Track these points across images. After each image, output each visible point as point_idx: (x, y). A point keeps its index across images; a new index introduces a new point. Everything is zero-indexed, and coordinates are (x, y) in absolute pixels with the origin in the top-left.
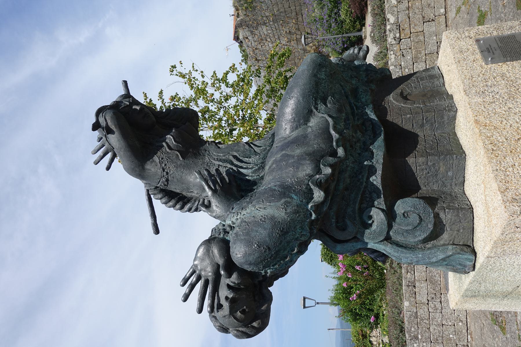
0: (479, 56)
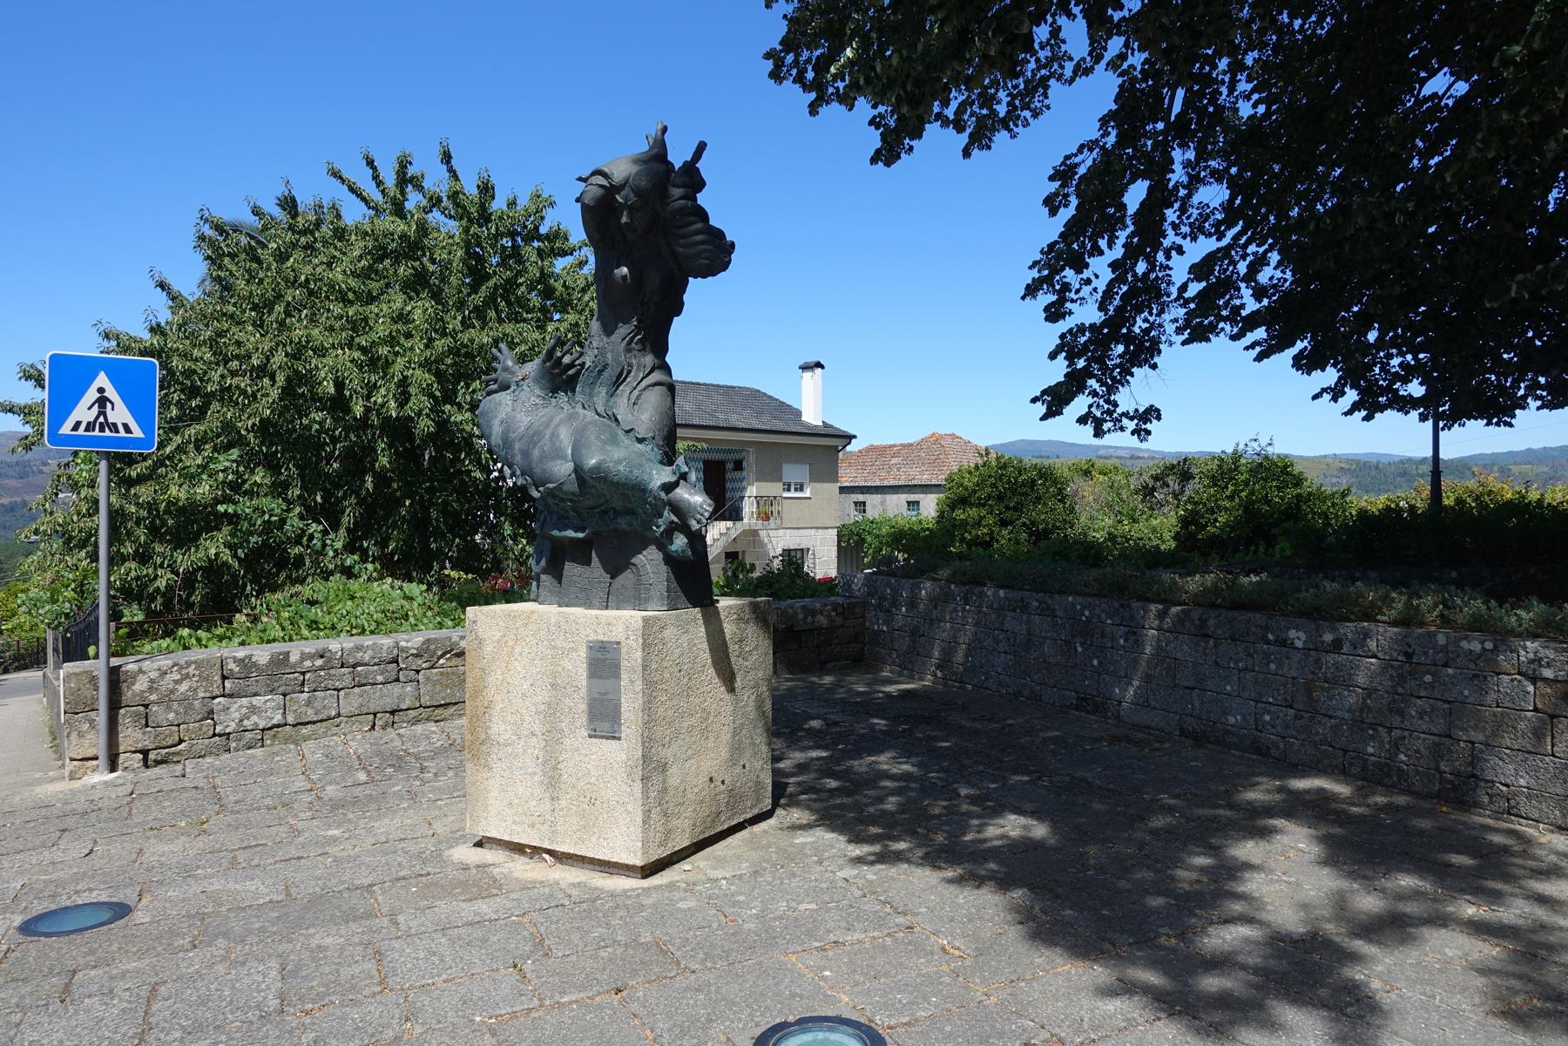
0: (601, 638)
